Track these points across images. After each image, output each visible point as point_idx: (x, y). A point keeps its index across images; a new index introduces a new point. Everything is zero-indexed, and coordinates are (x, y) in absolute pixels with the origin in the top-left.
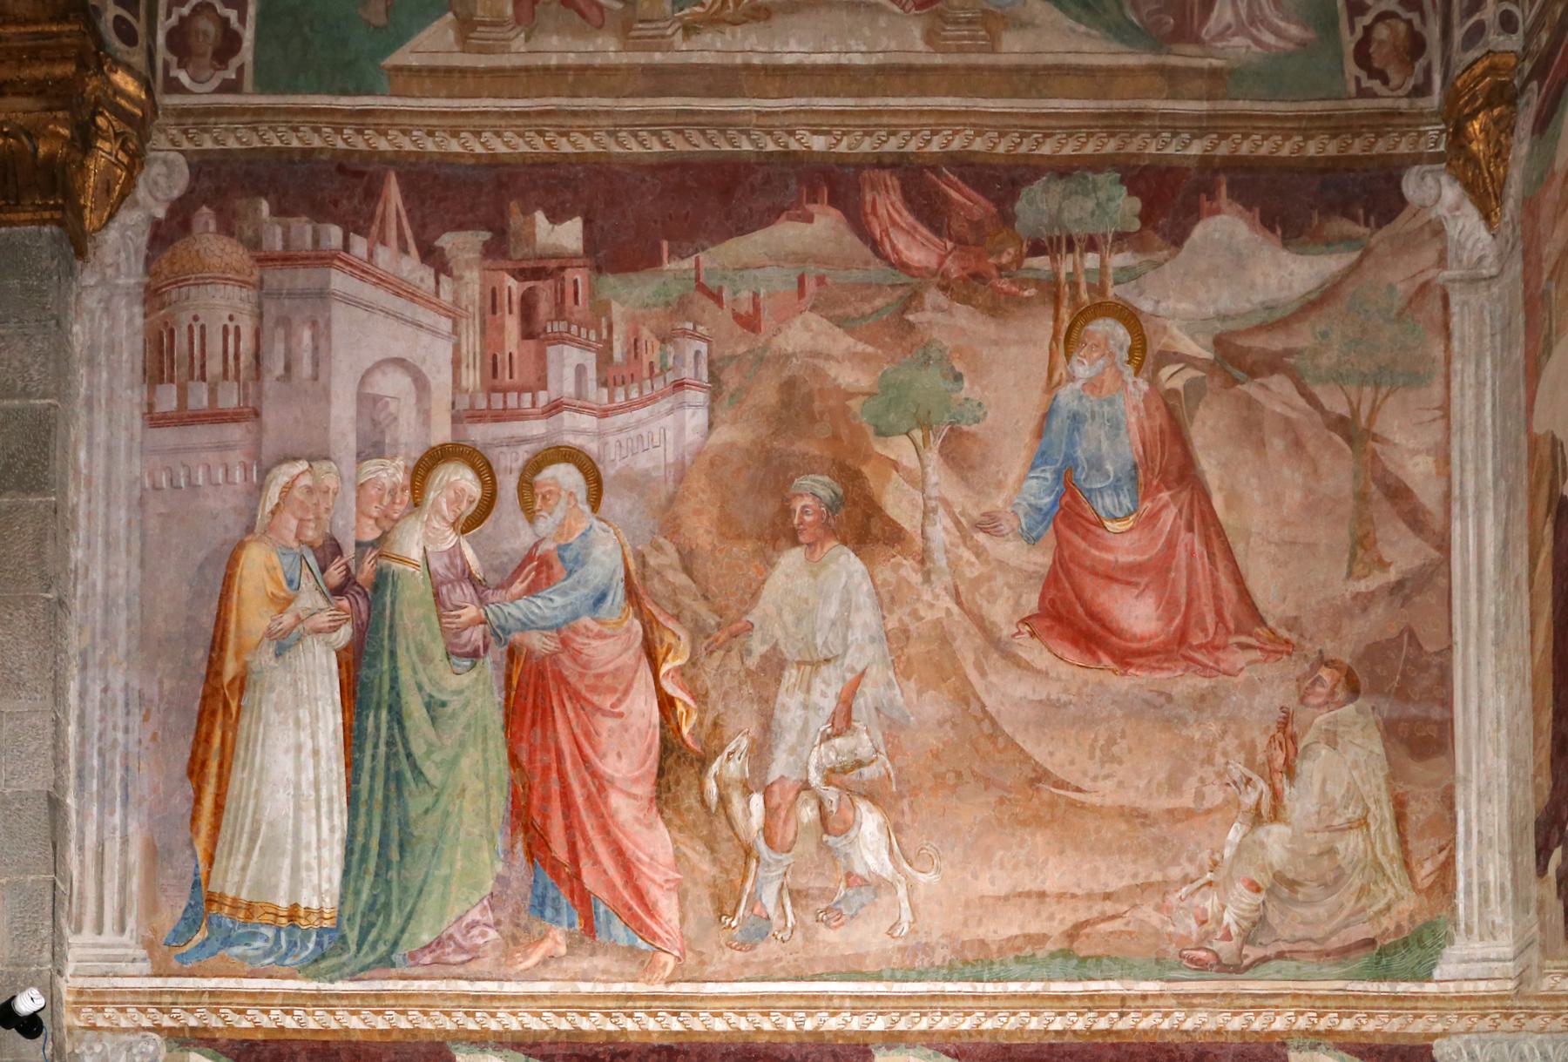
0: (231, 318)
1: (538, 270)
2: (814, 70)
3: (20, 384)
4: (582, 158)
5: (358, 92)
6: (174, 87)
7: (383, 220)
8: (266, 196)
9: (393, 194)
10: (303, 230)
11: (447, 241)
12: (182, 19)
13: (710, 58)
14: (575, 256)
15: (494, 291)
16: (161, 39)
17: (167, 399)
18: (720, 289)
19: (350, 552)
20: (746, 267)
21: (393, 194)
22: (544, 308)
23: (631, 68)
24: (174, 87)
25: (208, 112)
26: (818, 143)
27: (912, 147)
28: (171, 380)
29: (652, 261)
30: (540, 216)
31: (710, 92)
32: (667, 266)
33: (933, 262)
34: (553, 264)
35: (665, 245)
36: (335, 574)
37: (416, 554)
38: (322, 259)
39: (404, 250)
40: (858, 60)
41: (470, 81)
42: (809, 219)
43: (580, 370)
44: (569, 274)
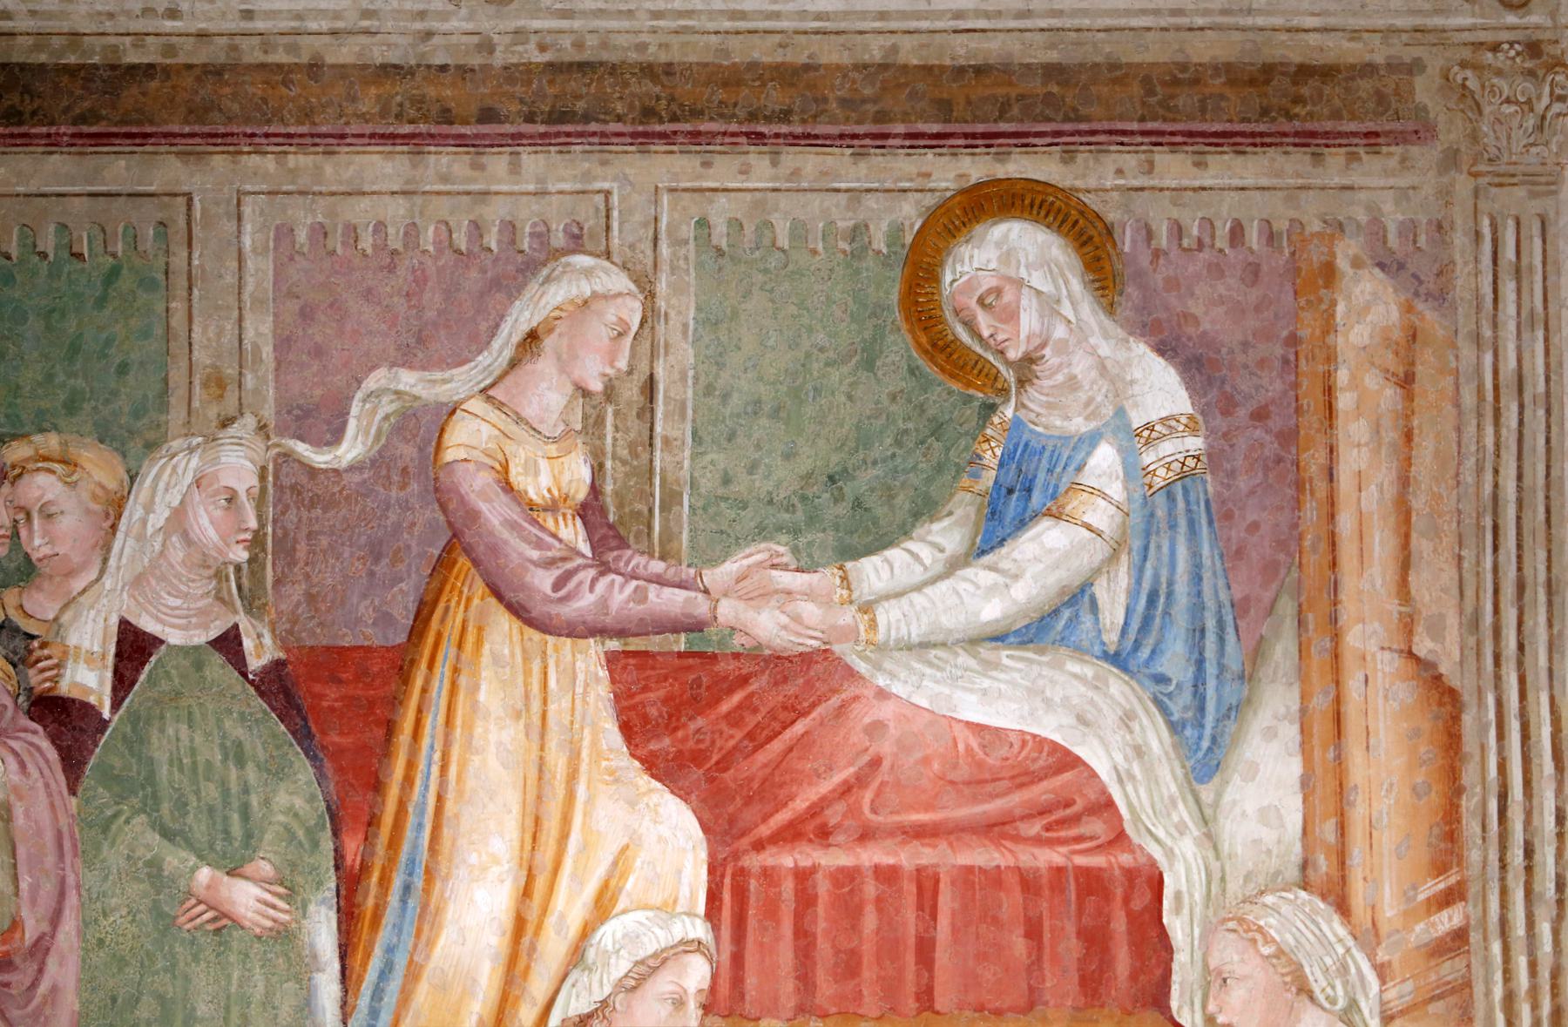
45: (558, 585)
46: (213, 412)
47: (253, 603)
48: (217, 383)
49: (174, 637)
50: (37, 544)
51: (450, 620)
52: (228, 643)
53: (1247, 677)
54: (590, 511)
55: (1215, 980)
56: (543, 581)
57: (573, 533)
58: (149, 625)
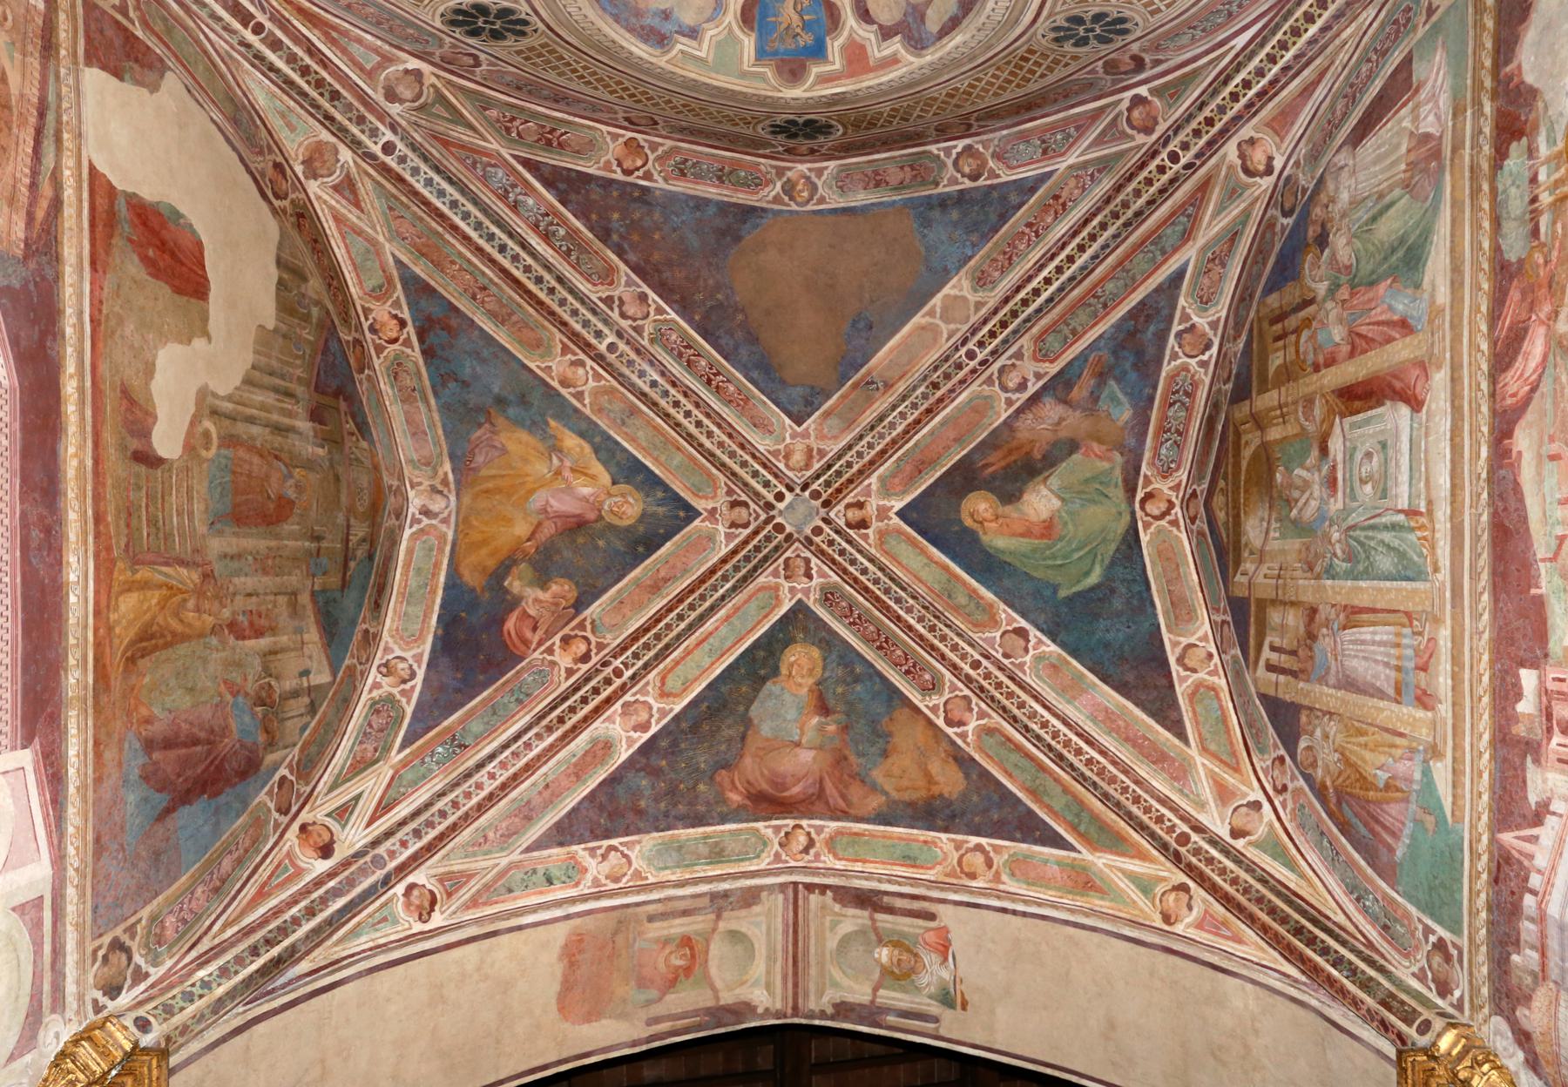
2: (1453, 461)
4: (1492, 662)
5: (1462, 850)
6: (1459, 1006)
7: (1520, 852)
8: (1509, 954)
9: (1507, 838)
10: (1528, 929)
12: (1434, 980)
13: (1448, 549)
14: (1540, 677)
15: (1560, 761)
16: (1439, 1002)
18: (1557, 537)
20: (1544, 513)
21: (1507, 838)
23: (1453, 618)
24: (1459, 1006)
25: (1471, 982)
26: (1484, 452)
27: (1485, 367)
29: (1540, 603)
32: (1543, 591)
33: (1542, 330)
34: (1544, 699)
35: (1533, 591)
38: (1541, 919)
39: (1534, 839)
41: (1458, 755)
42: (1520, 453)
44: (1551, 686)
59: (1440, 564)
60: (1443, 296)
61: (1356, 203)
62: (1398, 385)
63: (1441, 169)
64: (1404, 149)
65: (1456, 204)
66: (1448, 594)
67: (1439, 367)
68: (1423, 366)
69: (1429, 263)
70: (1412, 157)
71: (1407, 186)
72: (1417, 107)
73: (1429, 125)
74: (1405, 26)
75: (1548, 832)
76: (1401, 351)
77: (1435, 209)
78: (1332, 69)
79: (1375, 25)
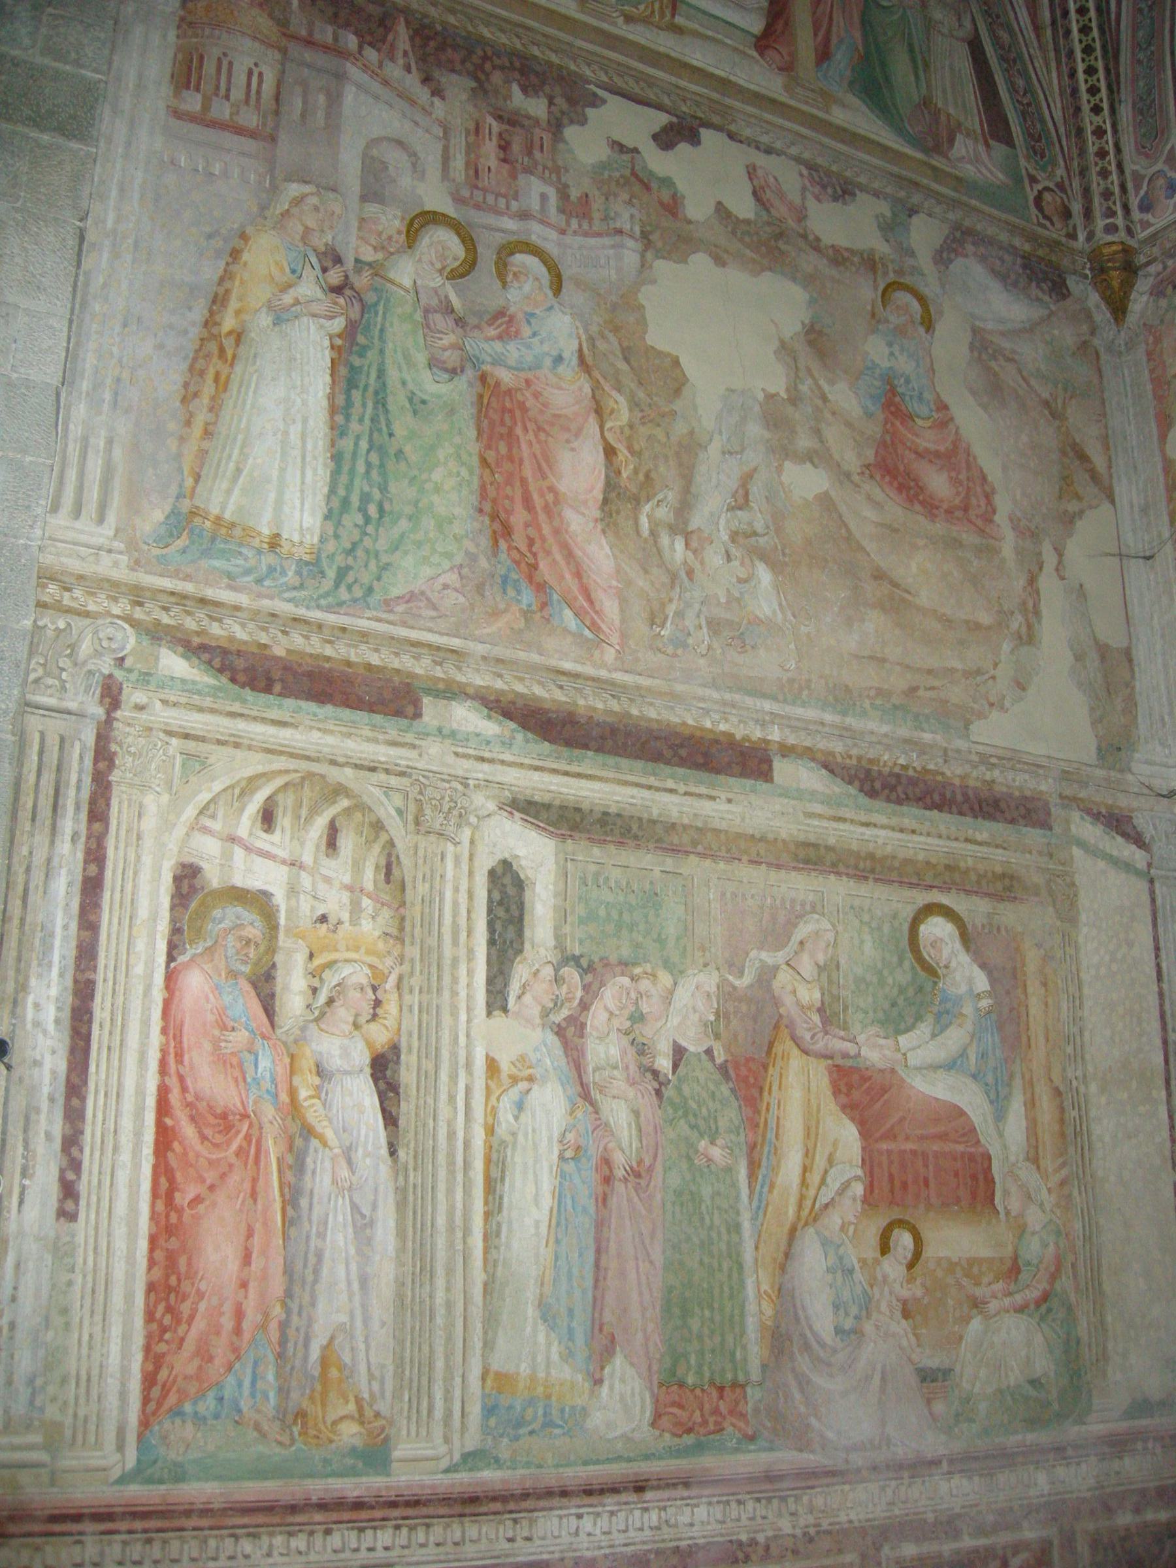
0: (256, 65)
1: (512, 120)
3: (73, 55)
11: (446, 79)
13: (643, 42)
17: (193, 102)
19: (350, 264)
22: (516, 148)
28: (198, 89)
30: (515, 88)
31: (641, 59)
36: (334, 277)
37: (407, 282)
40: (741, 82)
43: (544, 197)
45: (812, 1037)
46: (701, 961)
47: (717, 1036)
48: (703, 949)
49: (692, 1049)
50: (645, 1008)
51: (778, 1049)
52: (709, 1052)
53: (1009, 1085)
54: (821, 1010)
55: (1006, 1193)
56: (808, 1036)
57: (816, 1018)
58: (684, 1044)
59: (631, 27)
60: (838, 116)
61: (930, 25)
62: (780, 25)
63: (926, 150)
64: (951, 111)
65: (898, 157)
66: (605, 26)
67: (787, 88)
68: (787, 68)
69: (864, 108)
70: (943, 118)
71: (926, 102)
72: (976, 140)
73: (962, 147)
74: (1033, 147)
75: (412, 82)
76: (805, 42)
77: (900, 131)
78: (1036, 44)
79: (1046, 112)
